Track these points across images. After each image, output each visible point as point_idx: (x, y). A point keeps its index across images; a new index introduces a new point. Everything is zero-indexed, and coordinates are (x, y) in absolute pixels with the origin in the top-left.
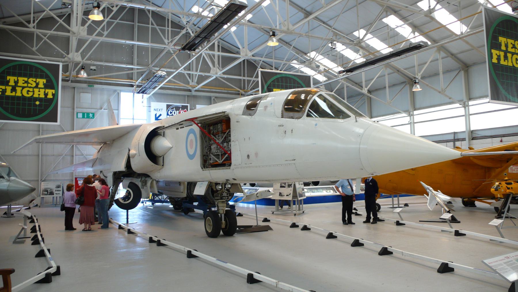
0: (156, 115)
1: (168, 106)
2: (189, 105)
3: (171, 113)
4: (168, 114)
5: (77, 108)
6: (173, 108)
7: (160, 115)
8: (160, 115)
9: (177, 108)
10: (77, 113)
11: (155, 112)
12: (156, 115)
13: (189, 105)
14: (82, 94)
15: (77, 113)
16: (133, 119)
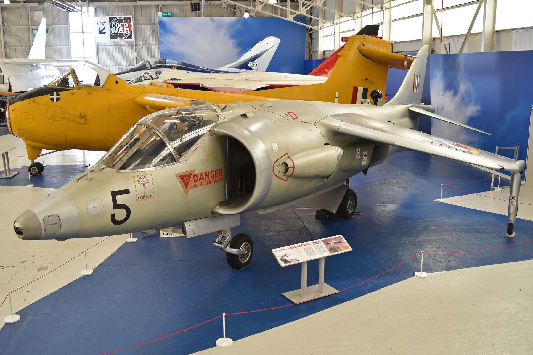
0: (99, 29)
1: (111, 19)
2: (131, 16)
3: (114, 25)
4: (111, 27)
5: (32, 25)
6: (115, 21)
7: (104, 28)
8: (104, 28)
9: (120, 21)
10: (33, 30)
11: (99, 26)
12: (99, 29)
13: (131, 16)
14: (35, 12)
15: (33, 30)
16: (83, 32)
